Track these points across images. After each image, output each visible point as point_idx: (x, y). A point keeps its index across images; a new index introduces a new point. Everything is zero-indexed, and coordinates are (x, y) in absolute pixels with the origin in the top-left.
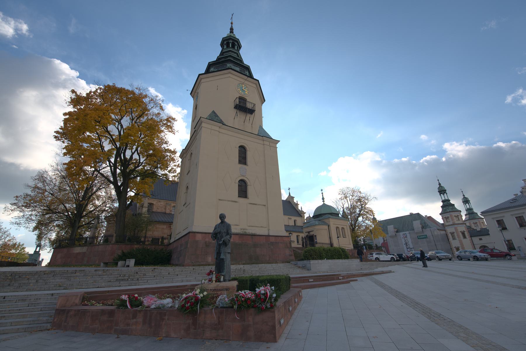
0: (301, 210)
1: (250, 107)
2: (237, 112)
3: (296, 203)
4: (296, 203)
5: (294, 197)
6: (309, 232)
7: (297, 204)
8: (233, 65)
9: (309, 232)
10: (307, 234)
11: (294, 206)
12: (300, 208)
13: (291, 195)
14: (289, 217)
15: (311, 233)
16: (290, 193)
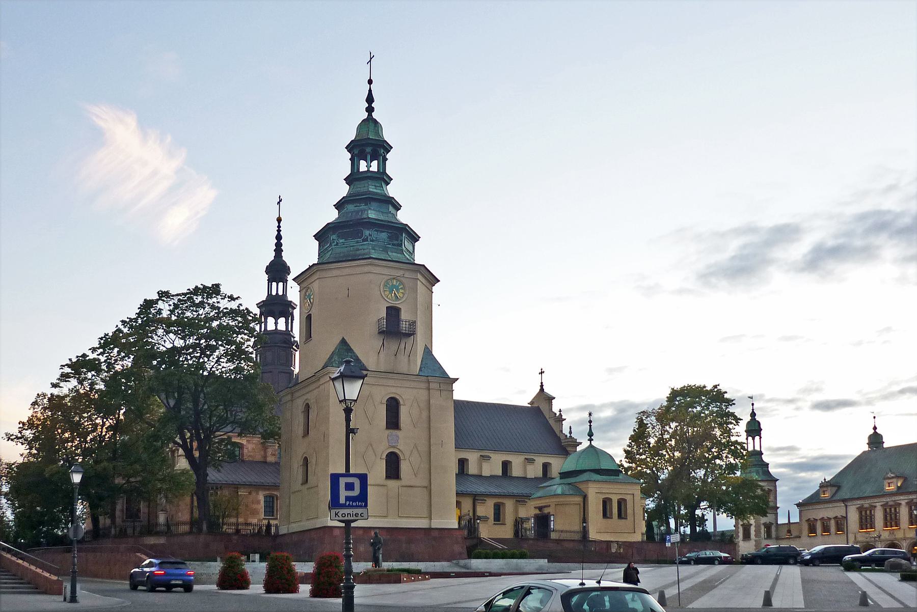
0: (568, 435)
1: (407, 329)
2: (383, 343)
3: (558, 415)
4: (558, 415)
5: (554, 398)
6: (542, 509)
7: (560, 419)
8: (376, 231)
9: (540, 508)
10: (537, 512)
11: (551, 422)
12: (566, 431)
13: (546, 390)
14: (526, 457)
15: (546, 511)
16: (542, 386)
